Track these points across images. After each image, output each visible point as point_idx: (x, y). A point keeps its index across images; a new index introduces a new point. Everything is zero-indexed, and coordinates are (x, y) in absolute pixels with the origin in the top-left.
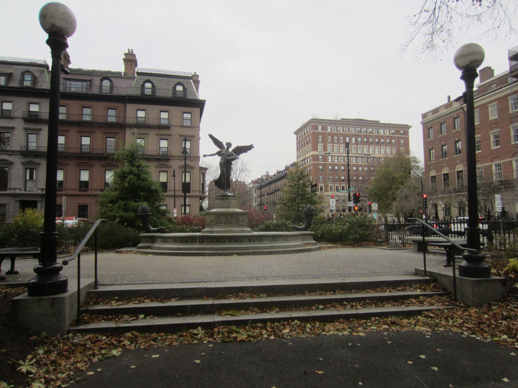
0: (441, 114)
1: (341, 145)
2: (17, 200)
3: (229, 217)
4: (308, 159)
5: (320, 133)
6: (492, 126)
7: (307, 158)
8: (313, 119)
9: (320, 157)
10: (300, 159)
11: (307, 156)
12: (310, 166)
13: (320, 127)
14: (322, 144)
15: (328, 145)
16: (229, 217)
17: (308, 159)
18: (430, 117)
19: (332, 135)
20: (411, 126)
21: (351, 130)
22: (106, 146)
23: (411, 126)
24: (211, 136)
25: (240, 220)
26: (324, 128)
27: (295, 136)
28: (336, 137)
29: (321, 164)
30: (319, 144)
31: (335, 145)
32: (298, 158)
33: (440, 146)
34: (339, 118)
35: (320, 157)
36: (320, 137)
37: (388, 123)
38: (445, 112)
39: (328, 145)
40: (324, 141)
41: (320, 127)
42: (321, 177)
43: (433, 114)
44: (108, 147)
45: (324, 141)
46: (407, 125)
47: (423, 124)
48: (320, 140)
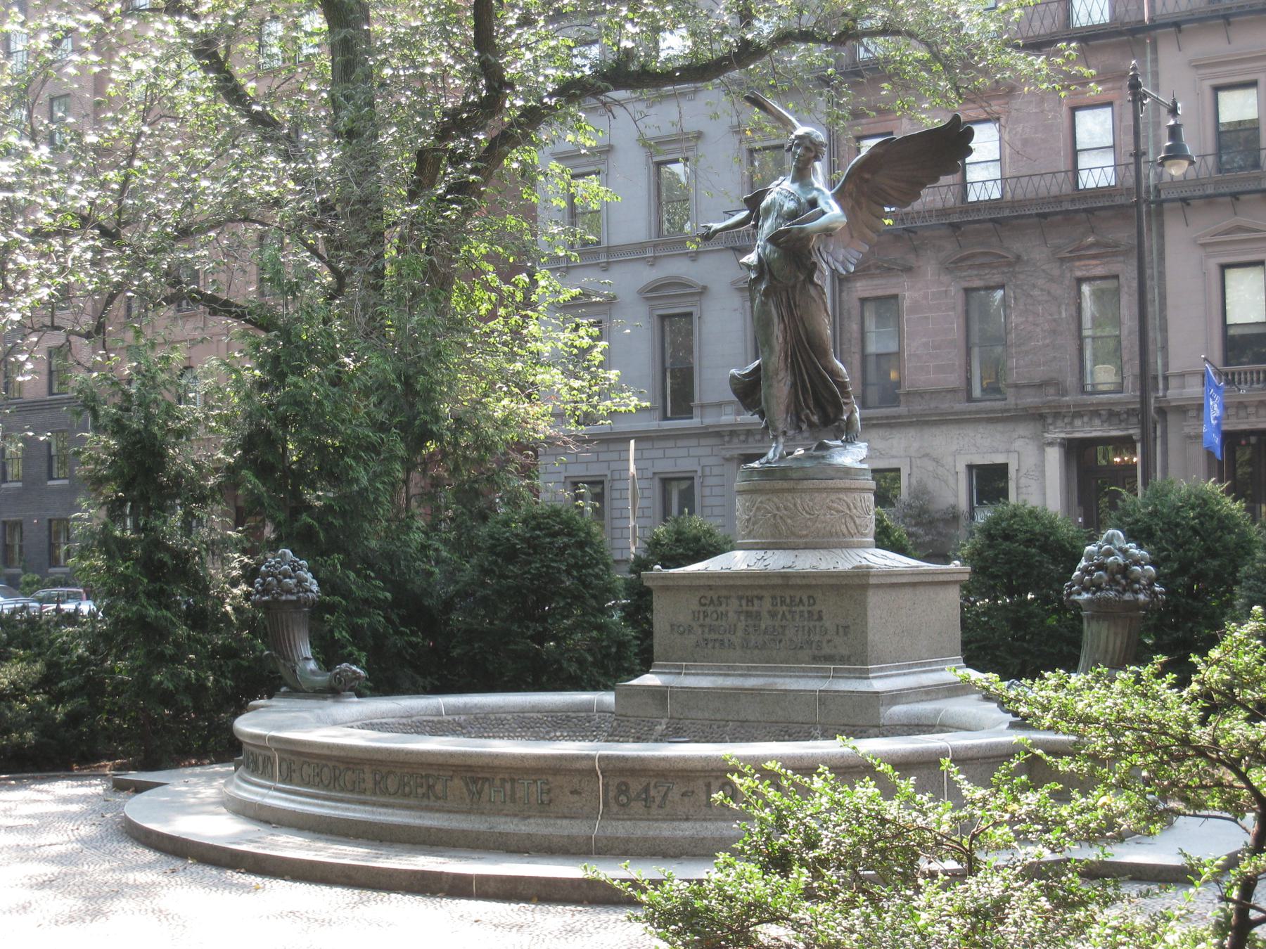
2: (728, 455)
3: (767, 605)
16: (767, 605)
22: (1075, 153)
25: (828, 623)
44: (1084, 161)
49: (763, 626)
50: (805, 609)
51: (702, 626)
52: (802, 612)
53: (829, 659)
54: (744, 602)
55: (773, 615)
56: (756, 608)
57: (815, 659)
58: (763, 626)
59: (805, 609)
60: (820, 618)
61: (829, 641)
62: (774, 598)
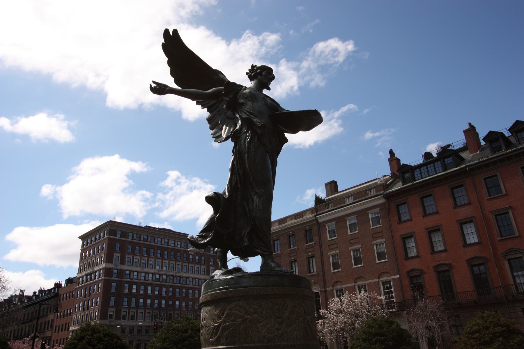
0: (290, 224)
1: (143, 258)
4: (97, 273)
5: (118, 241)
6: (352, 241)
7: (96, 272)
8: (111, 221)
9: (115, 271)
10: (83, 273)
11: (96, 269)
12: (97, 283)
14: (119, 255)
15: (127, 256)
17: (97, 273)
18: (275, 228)
19: (134, 245)
21: (156, 241)
26: (124, 234)
27: (80, 241)
28: (137, 248)
29: (115, 281)
30: (115, 254)
32: (80, 271)
34: (143, 225)
35: (115, 271)
36: (118, 245)
38: (296, 223)
39: (127, 256)
40: (123, 252)
42: (113, 299)
43: (280, 224)
45: (123, 252)
48: (118, 249)
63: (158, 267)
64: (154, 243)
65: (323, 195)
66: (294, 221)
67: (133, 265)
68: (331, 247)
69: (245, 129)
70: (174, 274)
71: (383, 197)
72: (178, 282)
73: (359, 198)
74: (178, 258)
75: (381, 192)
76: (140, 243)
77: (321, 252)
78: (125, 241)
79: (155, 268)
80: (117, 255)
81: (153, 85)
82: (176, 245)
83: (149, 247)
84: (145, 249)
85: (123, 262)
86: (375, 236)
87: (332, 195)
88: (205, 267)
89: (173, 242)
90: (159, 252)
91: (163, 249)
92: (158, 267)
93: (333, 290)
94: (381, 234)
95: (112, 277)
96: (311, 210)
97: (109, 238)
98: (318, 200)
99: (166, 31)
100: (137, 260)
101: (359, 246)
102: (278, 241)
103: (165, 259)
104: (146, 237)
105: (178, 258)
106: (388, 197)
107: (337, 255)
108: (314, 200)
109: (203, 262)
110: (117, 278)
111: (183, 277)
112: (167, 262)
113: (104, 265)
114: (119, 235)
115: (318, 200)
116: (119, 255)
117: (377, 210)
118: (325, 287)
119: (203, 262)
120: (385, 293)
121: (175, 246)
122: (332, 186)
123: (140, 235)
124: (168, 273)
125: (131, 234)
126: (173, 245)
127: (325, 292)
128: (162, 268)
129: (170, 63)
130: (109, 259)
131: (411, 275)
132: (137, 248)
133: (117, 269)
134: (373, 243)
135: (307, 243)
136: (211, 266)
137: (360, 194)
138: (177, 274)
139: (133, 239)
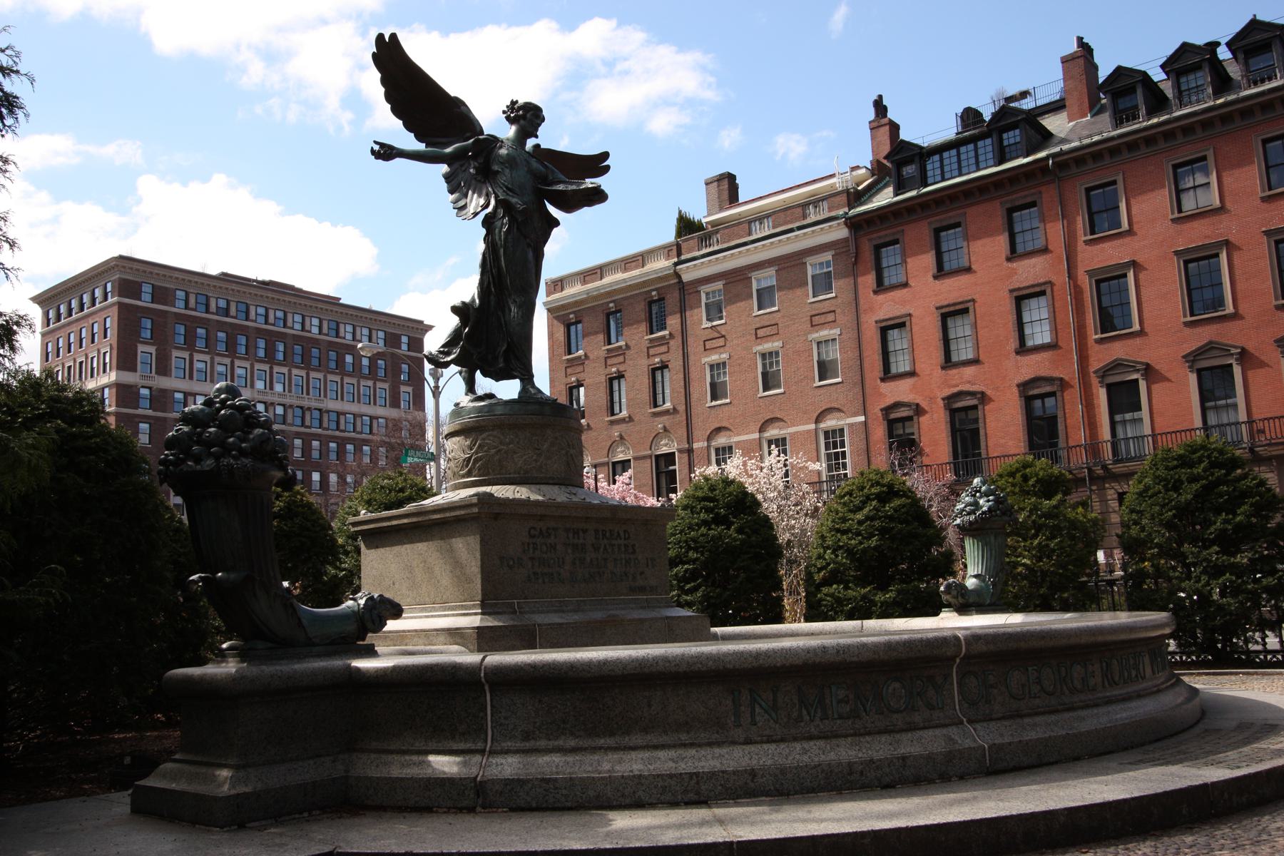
0: (611, 284)
1: (217, 359)
5: (146, 312)
6: (761, 333)
8: (121, 257)
13: (147, 289)
14: (152, 349)
15: (175, 353)
19: (191, 324)
20: (430, 327)
23: (430, 327)
24: (389, 56)
26: (161, 295)
28: (201, 331)
29: (145, 419)
30: (141, 348)
31: (197, 356)
33: (603, 379)
34: (214, 271)
36: (147, 323)
37: (367, 306)
39: (175, 353)
40: (161, 339)
41: (147, 289)
46: (421, 322)
47: (549, 310)
48: (148, 334)
49: (588, 560)
50: (622, 542)
51: (532, 559)
52: (619, 546)
53: (642, 590)
54: (571, 535)
55: (596, 549)
56: (581, 541)
57: (633, 590)
58: (588, 560)
59: (622, 542)
60: (634, 552)
61: (642, 573)
62: (596, 531)
63: (260, 385)
64: (247, 319)
65: (699, 212)
66: (620, 276)
67: (191, 378)
68: (709, 345)
69: (501, 212)
70: (306, 403)
71: (846, 223)
72: (316, 423)
73: (786, 223)
74: (315, 362)
75: (841, 212)
76: (208, 320)
77: (685, 356)
78: (166, 312)
79: (252, 386)
80: (146, 351)
81: (377, 148)
82: (307, 328)
83: (233, 332)
84: (221, 335)
85: (163, 368)
86: (816, 320)
87: (721, 209)
88: (386, 386)
89: (298, 318)
90: (262, 343)
91: (271, 338)
92: (260, 385)
93: (709, 447)
94: (830, 317)
95: (137, 407)
96: (665, 250)
97: (120, 304)
98: (686, 226)
99: (380, 37)
100: (202, 365)
101: (776, 344)
102: (580, 326)
103: (279, 364)
104: (222, 304)
105: (315, 362)
106: (855, 224)
107: (724, 363)
108: (675, 222)
109: (381, 373)
110: (150, 412)
111: (328, 412)
112: (285, 370)
113: (112, 377)
114: (147, 297)
115: (686, 226)
116: (152, 349)
117: (828, 256)
118: (690, 439)
119: (381, 373)
120: (829, 456)
121: (303, 329)
122: (727, 187)
123: (208, 298)
124: (288, 401)
125: (180, 294)
126: (298, 327)
127: (690, 451)
128: (271, 388)
129: (384, 82)
130: (126, 360)
131: (893, 416)
132: (201, 331)
133: (150, 388)
134: (811, 337)
135: (652, 333)
136: (405, 383)
137: (793, 213)
138: (314, 404)
139: (187, 307)
